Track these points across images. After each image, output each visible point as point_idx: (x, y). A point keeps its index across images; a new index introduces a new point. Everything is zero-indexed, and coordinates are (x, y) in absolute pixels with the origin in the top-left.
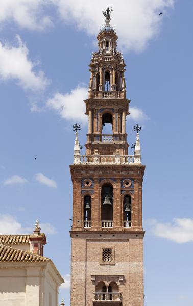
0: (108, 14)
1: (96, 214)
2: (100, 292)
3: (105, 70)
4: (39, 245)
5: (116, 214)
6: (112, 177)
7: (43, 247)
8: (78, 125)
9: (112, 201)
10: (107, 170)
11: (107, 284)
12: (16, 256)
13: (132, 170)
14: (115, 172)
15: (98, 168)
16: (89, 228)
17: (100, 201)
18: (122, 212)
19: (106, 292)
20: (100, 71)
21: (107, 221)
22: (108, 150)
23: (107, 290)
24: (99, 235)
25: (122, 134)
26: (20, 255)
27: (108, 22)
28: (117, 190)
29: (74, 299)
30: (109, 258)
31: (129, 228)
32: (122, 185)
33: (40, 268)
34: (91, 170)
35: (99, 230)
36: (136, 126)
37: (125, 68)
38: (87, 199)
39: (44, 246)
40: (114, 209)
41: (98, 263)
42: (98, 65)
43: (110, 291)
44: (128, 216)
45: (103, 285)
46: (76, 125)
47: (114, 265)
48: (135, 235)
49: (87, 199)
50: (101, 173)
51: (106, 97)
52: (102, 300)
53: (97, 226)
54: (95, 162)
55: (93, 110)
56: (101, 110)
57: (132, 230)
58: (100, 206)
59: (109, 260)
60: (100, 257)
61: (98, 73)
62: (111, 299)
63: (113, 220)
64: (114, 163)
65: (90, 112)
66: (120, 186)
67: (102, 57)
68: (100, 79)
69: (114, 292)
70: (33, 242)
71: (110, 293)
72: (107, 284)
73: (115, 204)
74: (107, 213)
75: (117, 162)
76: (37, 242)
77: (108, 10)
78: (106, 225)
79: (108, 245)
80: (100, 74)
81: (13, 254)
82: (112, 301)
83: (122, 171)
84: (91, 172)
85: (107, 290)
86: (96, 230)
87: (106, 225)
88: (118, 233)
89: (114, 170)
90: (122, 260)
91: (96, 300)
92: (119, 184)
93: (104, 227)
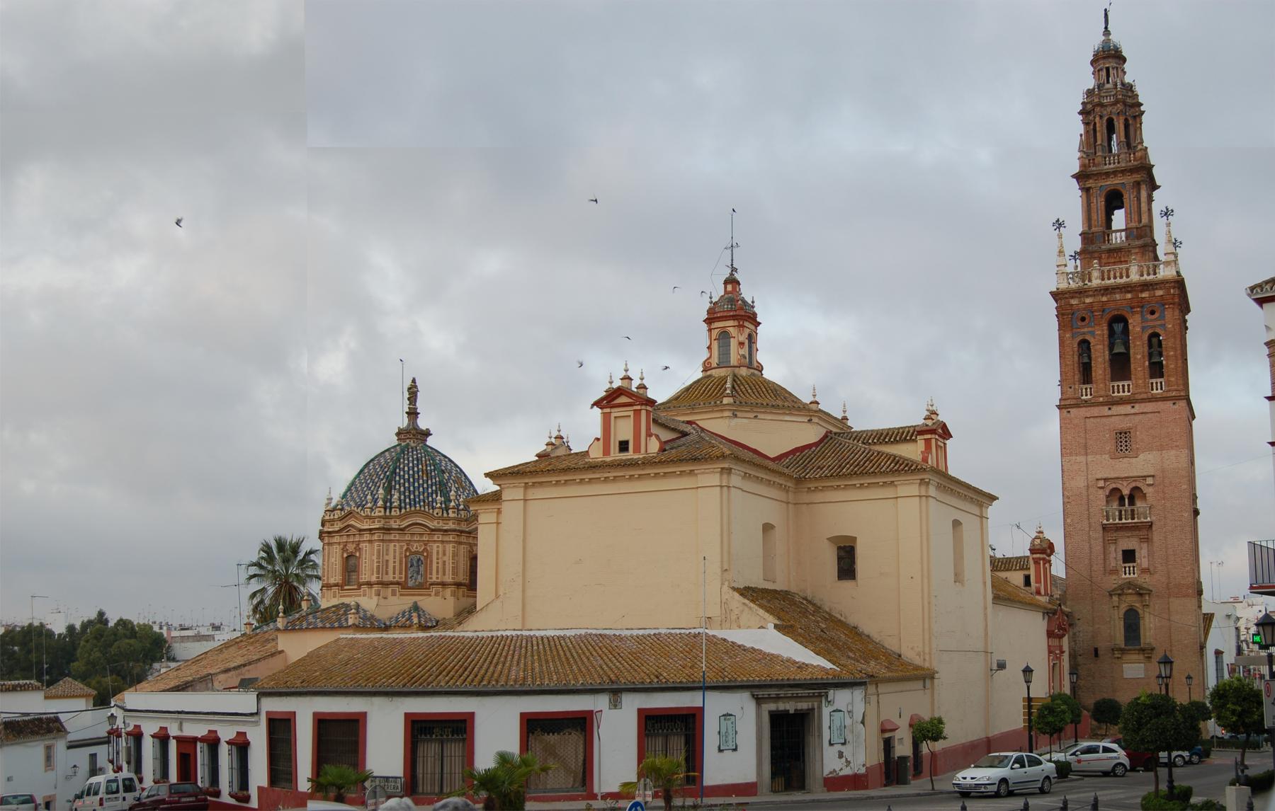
1: (1101, 372)
2: (1115, 505)
4: (933, 441)
5: (1136, 369)
7: (945, 444)
8: (1061, 221)
9: (1126, 345)
10: (1115, 293)
11: (1126, 492)
13: (1161, 289)
14: (1129, 296)
15: (1100, 290)
16: (1089, 397)
17: (1107, 349)
18: (1147, 363)
19: (1124, 506)
21: (1121, 384)
22: (1118, 255)
23: (1127, 500)
25: (1141, 225)
28: (1134, 326)
29: (1069, 521)
30: (1126, 446)
31: (1159, 391)
32: (1142, 316)
34: (1087, 297)
35: (1106, 399)
38: (1085, 345)
39: (947, 442)
40: (1132, 360)
41: (1108, 456)
43: (1132, 502)
44: (1157, 370)
45: (1118, 495)
46: (1058, 220)
48: (1172, 402)
49: (1085, 345)
50: (1104, 299)
51: (1110, 164)
52: (1117, 521)
53: (1102, 393)
54: (1096, 282)
57: (1165, 395)
58: (1107, 357)
59: (1127, 450)
60: (1110, 446)
62: (1133, 519)
64: (1128, 280)
66: (1140, 319)
67: (1100, 97)
68: (1098, 134)
69: (1139, 504)
70: (922, 437)
71: (1132, 507)
72: (1126, 492)
73: (1132, 351)
74: (1120, 366)
75: (1134, 277)
76: (928, 436)
78: (1086, 392)
79: (1124, 424)
82: (1136, 520)
84: (1088, 300)
85: (1127, 500)
86: (1101, 399)
87: (1086, 392)
88: (1140, 403)
89: (1129, 292)
90: (1151, 449)
91: (1108, 520)
92: (1138, 318)
93: (1116, 394)
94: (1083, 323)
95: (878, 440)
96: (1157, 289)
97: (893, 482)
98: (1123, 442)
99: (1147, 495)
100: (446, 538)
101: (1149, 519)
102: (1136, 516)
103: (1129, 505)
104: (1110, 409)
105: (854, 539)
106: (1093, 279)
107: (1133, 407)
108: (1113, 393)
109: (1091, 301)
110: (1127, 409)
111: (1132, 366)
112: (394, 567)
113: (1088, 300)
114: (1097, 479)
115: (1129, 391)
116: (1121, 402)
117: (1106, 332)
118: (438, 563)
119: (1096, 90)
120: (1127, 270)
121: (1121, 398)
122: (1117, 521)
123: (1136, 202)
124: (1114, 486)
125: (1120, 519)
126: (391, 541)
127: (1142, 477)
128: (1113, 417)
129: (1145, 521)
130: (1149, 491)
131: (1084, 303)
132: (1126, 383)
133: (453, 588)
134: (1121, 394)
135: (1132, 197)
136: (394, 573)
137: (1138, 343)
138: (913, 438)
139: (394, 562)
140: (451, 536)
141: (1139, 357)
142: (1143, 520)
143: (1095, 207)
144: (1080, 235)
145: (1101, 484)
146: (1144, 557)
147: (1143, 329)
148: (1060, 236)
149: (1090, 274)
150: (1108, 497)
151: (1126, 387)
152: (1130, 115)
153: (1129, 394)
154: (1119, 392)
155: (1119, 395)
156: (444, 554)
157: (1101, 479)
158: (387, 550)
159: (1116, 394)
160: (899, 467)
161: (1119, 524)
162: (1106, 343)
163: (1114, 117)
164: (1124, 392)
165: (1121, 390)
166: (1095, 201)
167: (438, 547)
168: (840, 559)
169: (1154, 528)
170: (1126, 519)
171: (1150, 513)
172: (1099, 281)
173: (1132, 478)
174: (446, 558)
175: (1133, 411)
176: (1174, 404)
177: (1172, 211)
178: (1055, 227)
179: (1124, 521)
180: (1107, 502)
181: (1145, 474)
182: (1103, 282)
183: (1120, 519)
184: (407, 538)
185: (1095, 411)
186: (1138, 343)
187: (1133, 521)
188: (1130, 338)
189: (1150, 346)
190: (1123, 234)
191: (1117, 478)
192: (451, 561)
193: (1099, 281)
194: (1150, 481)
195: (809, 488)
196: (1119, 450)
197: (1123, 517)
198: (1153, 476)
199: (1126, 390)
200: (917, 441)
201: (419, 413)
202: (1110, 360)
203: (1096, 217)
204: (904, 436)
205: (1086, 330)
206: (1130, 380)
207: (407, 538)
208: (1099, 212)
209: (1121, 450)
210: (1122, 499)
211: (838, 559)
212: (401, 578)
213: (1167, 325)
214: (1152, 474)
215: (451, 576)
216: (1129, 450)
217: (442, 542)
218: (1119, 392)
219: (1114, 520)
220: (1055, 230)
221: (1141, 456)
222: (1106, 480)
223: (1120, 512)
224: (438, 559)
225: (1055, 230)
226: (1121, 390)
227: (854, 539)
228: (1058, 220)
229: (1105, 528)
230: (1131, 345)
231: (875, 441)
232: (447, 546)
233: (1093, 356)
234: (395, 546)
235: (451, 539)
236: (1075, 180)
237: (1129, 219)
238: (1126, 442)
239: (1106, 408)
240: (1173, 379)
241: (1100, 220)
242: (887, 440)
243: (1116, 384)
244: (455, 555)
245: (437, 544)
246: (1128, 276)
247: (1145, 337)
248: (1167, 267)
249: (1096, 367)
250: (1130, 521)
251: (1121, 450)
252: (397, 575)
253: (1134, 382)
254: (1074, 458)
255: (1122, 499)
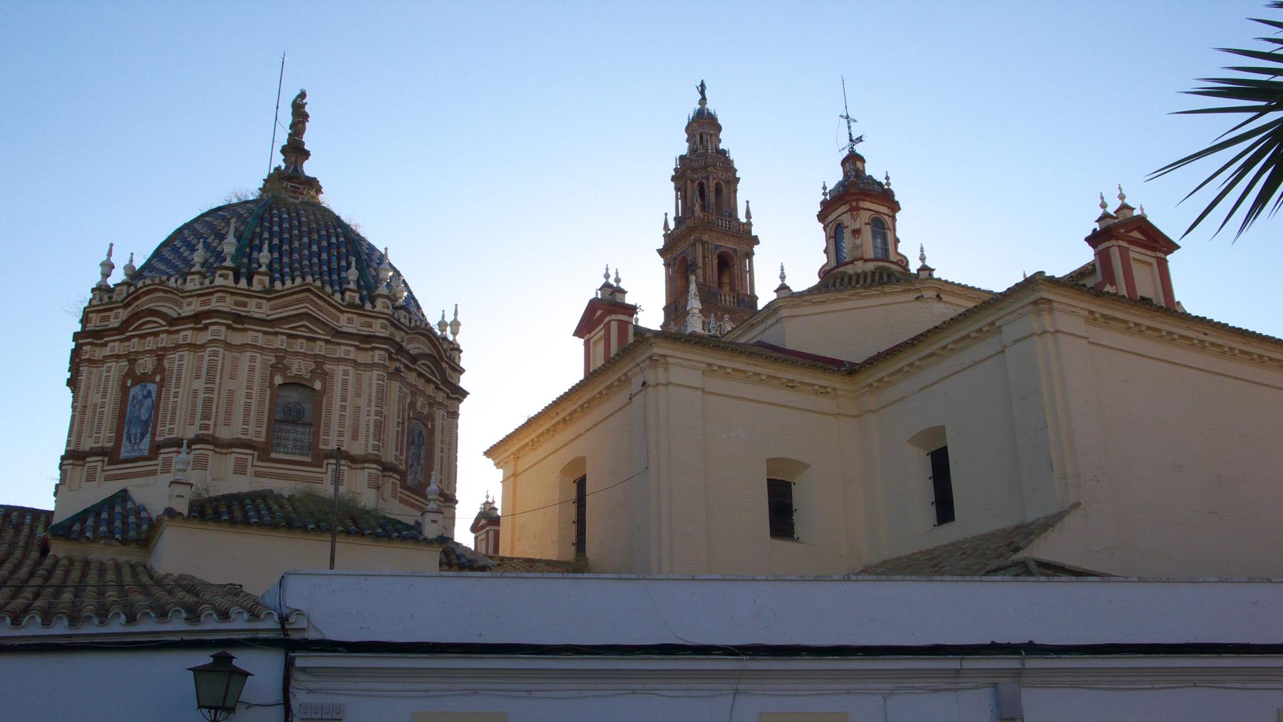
100: (364, 358)
112: (248, 406)
118: (343, 408)
126: (243, 347)
133: (373, 469)
136: (246, 422)
139: (249, 396)
140: (377, 353)
156: (358, 395)
158: (235, 367)
167: (346, 373)
174: (362, 402)
184: (279, 342)
192: (373, 409)
201: (264, 180)
207: (279, 342)
212: (258, 433)
215: (371, 442)
217: (355, 363)
224: (344, 399)
232: (366, 375)
234: (253, 359)
235: (377, 361)
244: (382, 394)
245: (342, 368)
252: (252, 428)
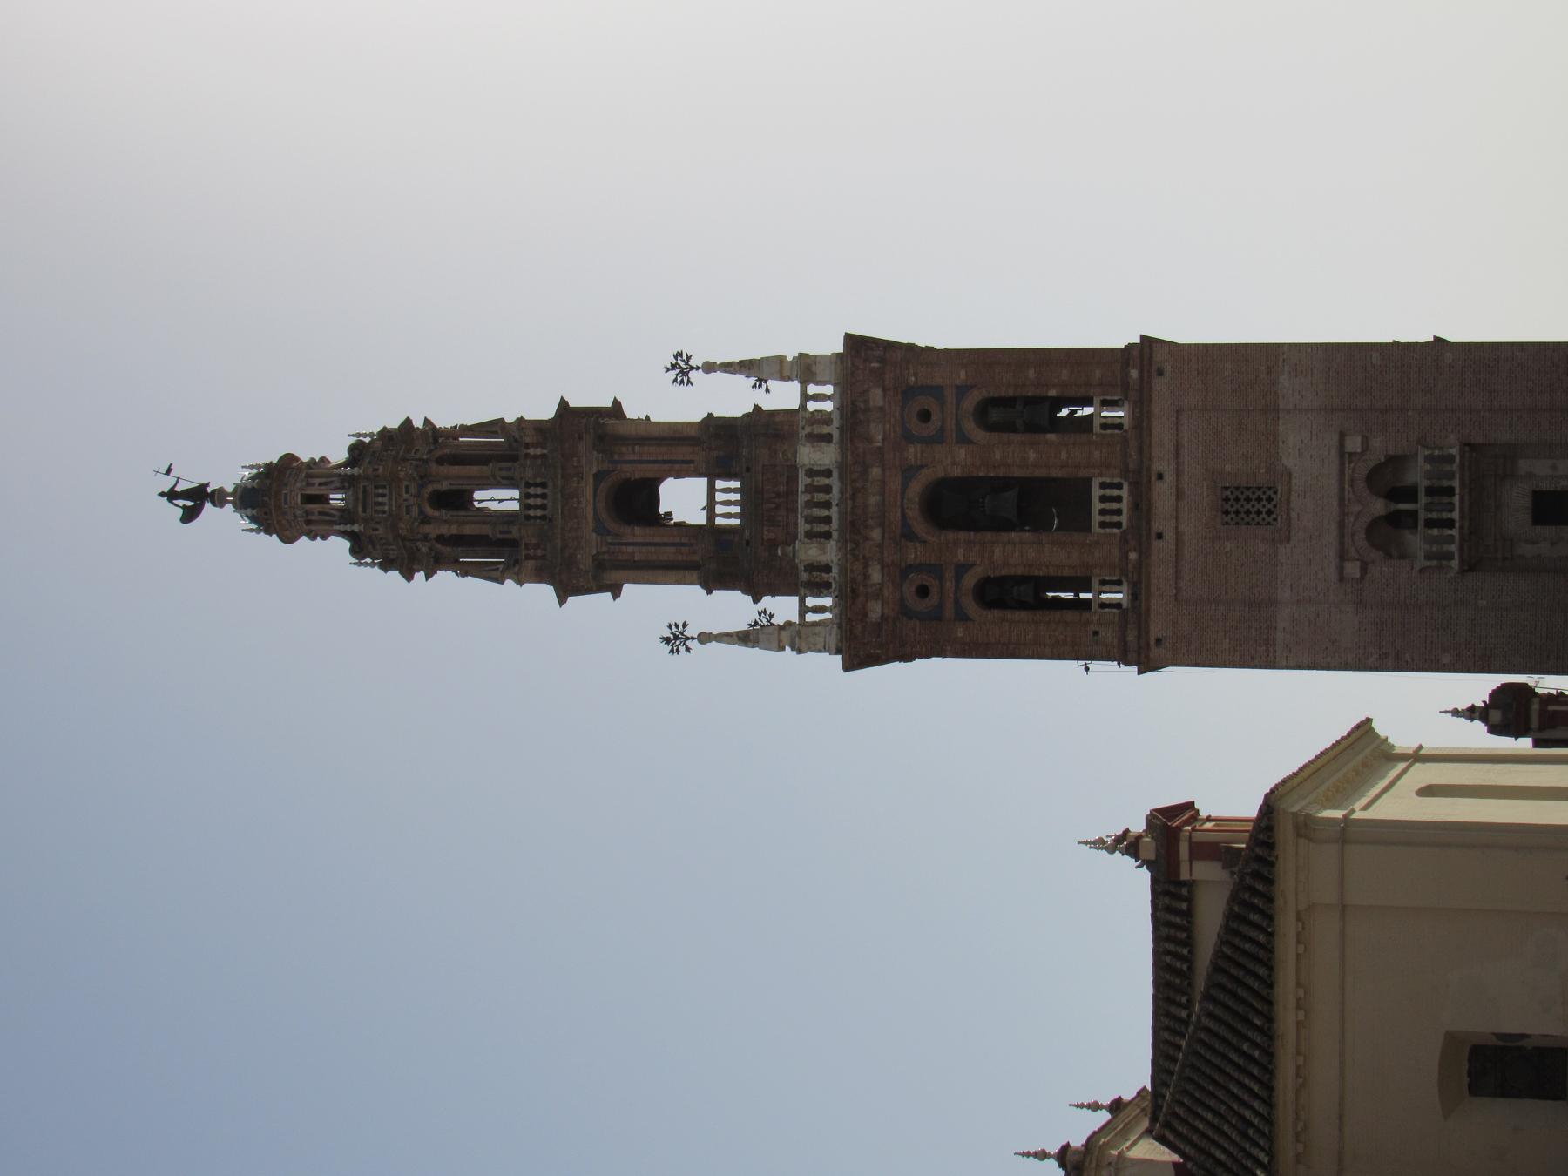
0: (186, 494)
3: (429, 511)
6: (895, 483)
7: (1209, 819)
8: (667, 633)
11: (1378, 507)
12: (1247, 946)
14: (876, 471)
19: (1416, 512)
20: (427, 529)
21: (1097, 505)
23: (1402, 506)
24: (1157, 544)
26: (1245, 929)
27: (218, 498)
28: (954, 463)
30: (1259, 500)
33: (1302, 841)
34: (866, 576)
36: (673, 374)
37: (418, 423)
40: (1039, 473)
42: (404, 539)
43: (1410, 494)
46: (667, 640)
47: (1290, 475)
50: (876, 534)
52: (1455, 532)
54: (830, 553)
55: (600, 566)
56: (600, 529)
59: (1270, 500)
61: (441, 539)
62: (1450, 491)
63: (1087, 483)
64: (835, 474)
65: (613, 576)
69: (1418, 475)
72: (1378, 507)
77: (172, 495)
80: (445, 530)
81: (1240, 959)
82: (1456, 484)
83: (870, 440)
85: (1402, 506)
91: (1450, 557)
94: (934, 590)
95: (1185, 994)
96: (866, 402)
97: (1298, 913)
98: (1249, 506)
99: (1391, 453)
101: (1454, 451)
102: (1445, 483)
103: (1415, 499)
104: (1160, 536)
105: (1452, 1039)
106: (823, 559)
107: (1160, 476)
108: (1118, 525)
109: (879, 567)
110: (1163, 496)
111: (1055, 473)
113: (876, 575)
114: (1341, 579)
115: (1119, 486)
116: (1142, 506)
117: (962, 535)
119: (356, 528)
120: (811, 473)
121: (1136, 506)
122: (1455, 532)
123: (646, 448)
124: (1360, 537)
125: (1450, 524)
127: (1342, 464)
128: (1182, 527)
129: (1457, 459)
130: (1380, 447)
131: (880, 546)
132: (1097, 492)
134: (1124, 505)
135: (632, 457)
137: (998, 456)
138: (1184, 891)
141: (1032, 455)
142: (1455, 467)
143: (644, 549)
144: (709, 592)
145: (1353, 569)
146: (1554, 468)
147: (963, 439)
148: (704, 638)
149: (811, 568)
150: (1389, 556)
151: (1109, 492)
152: (430, 451)
153: (1126, 486)
154: (1119, 512)
155: (1125, 511)
157: (1341, 570)
159: (1124, 519)
160: (1262, 1149)
161: (1461, 527)
162: (989, 536)
163: (430, 488)
164: (1119, 499)
165: (1115, 506)
166: (630, 549)
168: (1504, 1091)
169: (1480, 440)
170: (1452, 510)
171: (1441, 448)
172: (832, 545)
173: (1342, 489)
175: (1169, 477)
176: (1160, 373)
177: (680, 354)
178: (682, 649)
179: (1456, 515)
180: (1402, 557)
181: (1334, 453)
182: (835, 535)
183: (1450, 524)
185: (1161, 573)
186: (998, 456)
187: (1457, 491)
188: (981, 474)
189: (1009, 427)
190: (720, 484)
191: (1341, 526)
193: (832, 545)
194: (1354, 444)
195: (1298, 1159)
196: (1270, 519)
197: (1445, 515)
198: (1342, 435)
199: (1115, 492)
200: (1194, 881)
202: (1034, 530)
203: (672, 549)
204: (1178, 920)
205: (949, 585)
206: (1091, 479)
208: (657, 540)
209: (1269, 513)
210: (1396, 521)
211: (1503, 1095)
213: (958, 383)
214: (1336, 438)
216: (1270, 493)
218: (1119, 512)
219: (1450, 539)
220: (688, 649)
221: (1289, 462)
222: (1342, 556)
223: (1430, 524)
225: (688, 649)
226: (1115, 506)
227: (1452, 1039)
228: (667, 640)
229: (1469, 567)
230: (1002, 472)
231: (1184, 1000)
233: (1020, 571)
236: (570, 599)
237: (685, 466)
238: (1248, 500)
239: (1157, 544)
240: (1098, 373)
241: (677, 540)
242: (1185, 967)
243: (1096, 518)
246: (827, 473)
247: (980, 435)
248: (814, 374)
249: (1047, 567)
250: (1456, 499)
251: (1269, 513)
253: (1097, 471)
254: (1280, 636)
255: (1396, 521)
